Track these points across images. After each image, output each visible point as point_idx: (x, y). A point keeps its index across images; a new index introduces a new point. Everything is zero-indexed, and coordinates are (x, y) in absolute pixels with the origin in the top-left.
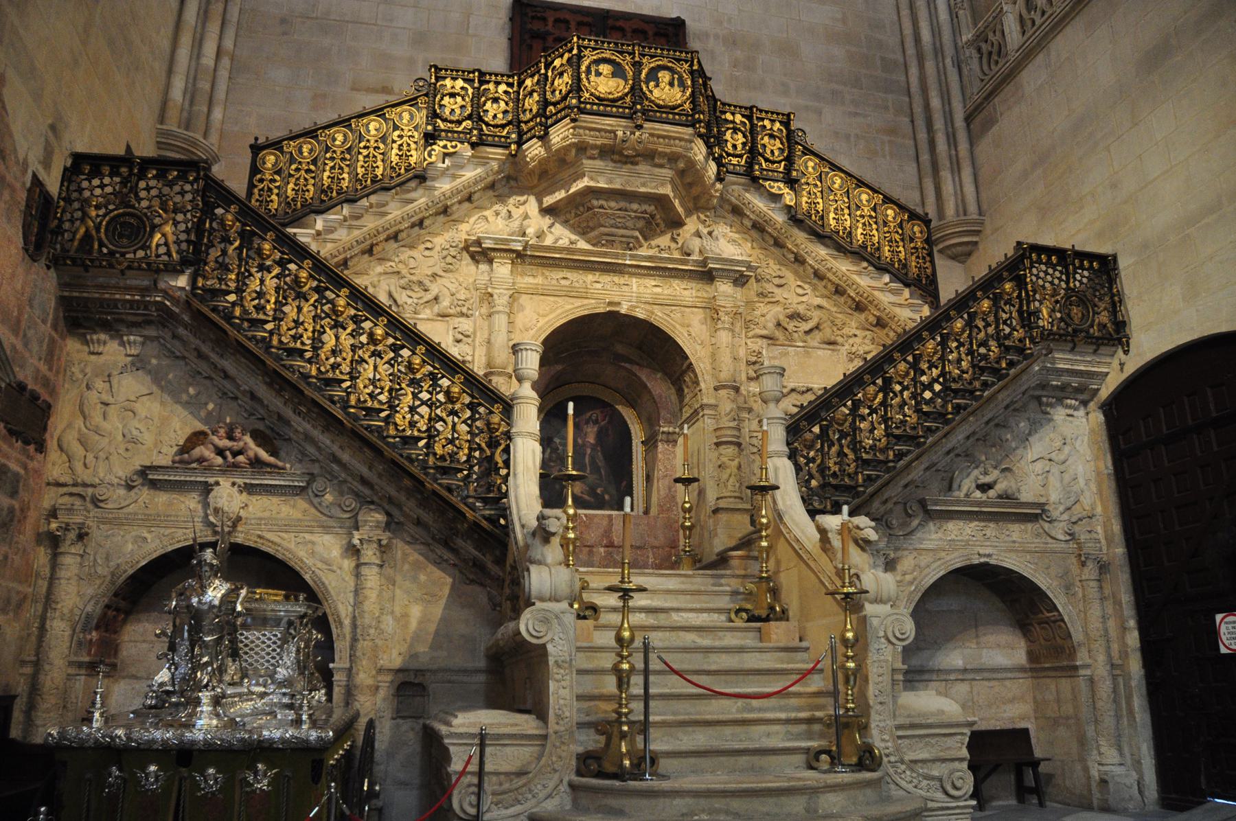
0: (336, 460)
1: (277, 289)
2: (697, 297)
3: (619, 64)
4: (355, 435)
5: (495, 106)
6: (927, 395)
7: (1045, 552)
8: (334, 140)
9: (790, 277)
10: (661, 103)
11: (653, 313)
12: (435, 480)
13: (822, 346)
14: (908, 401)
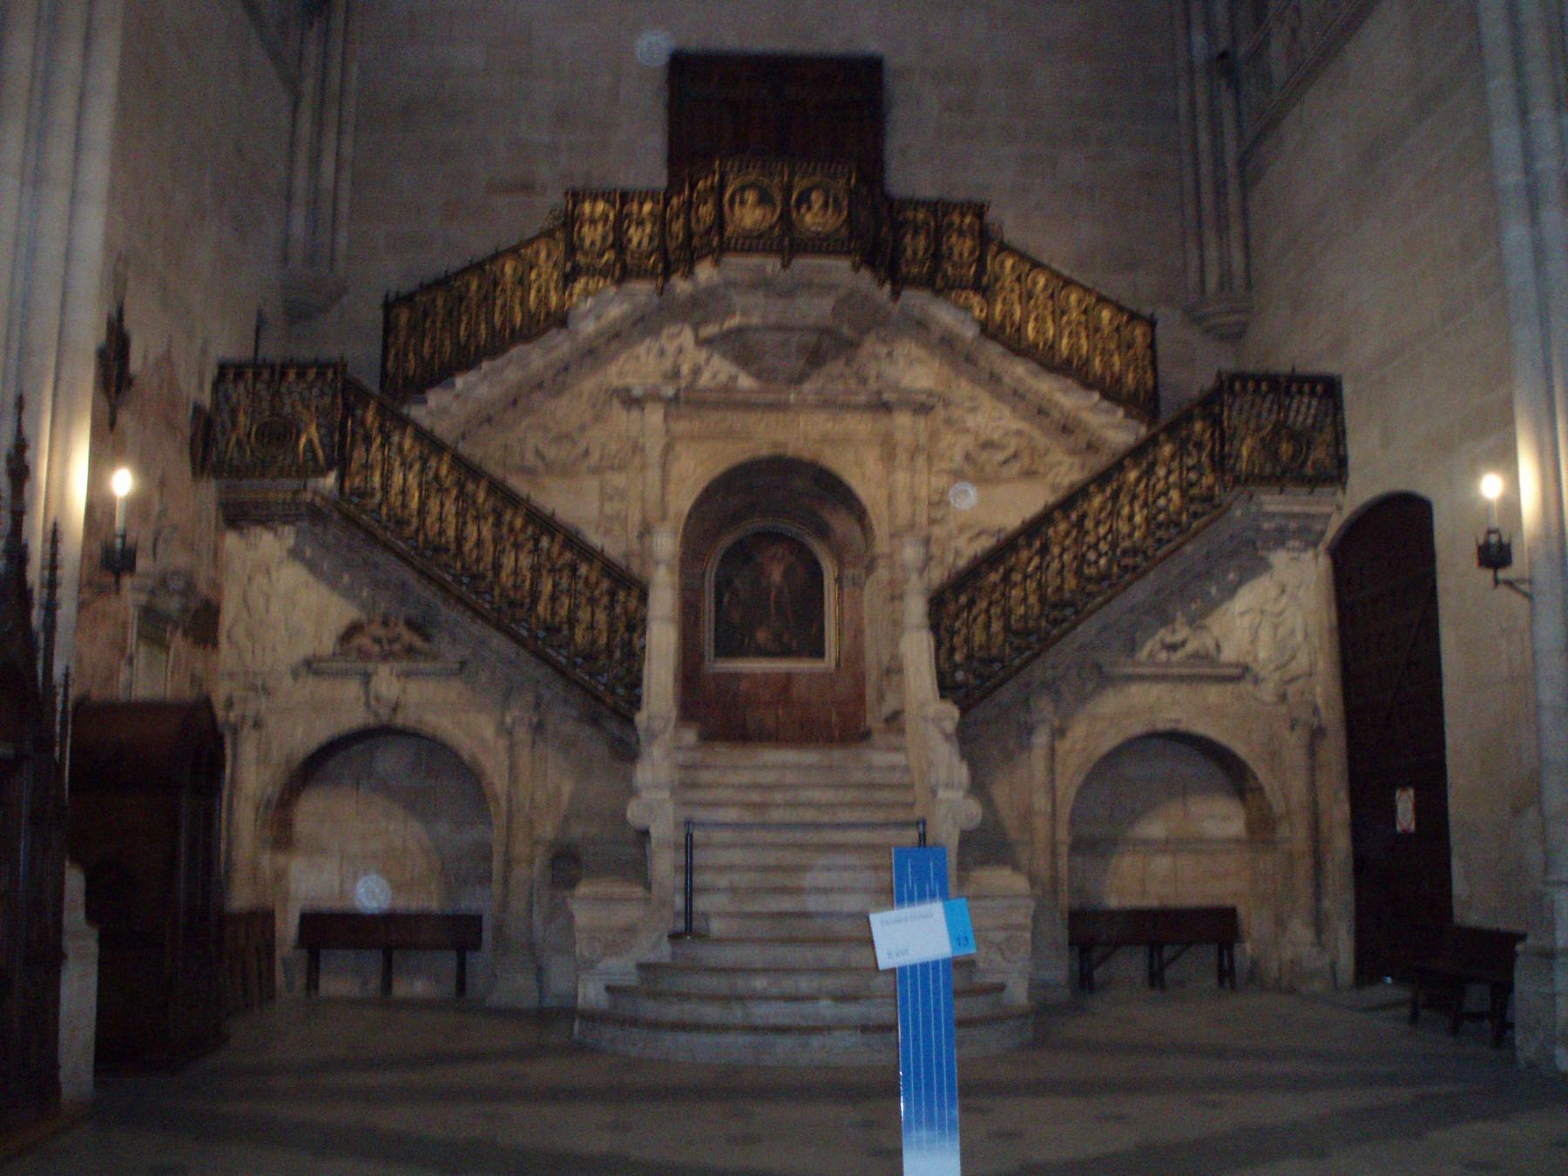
9: (986, 401)
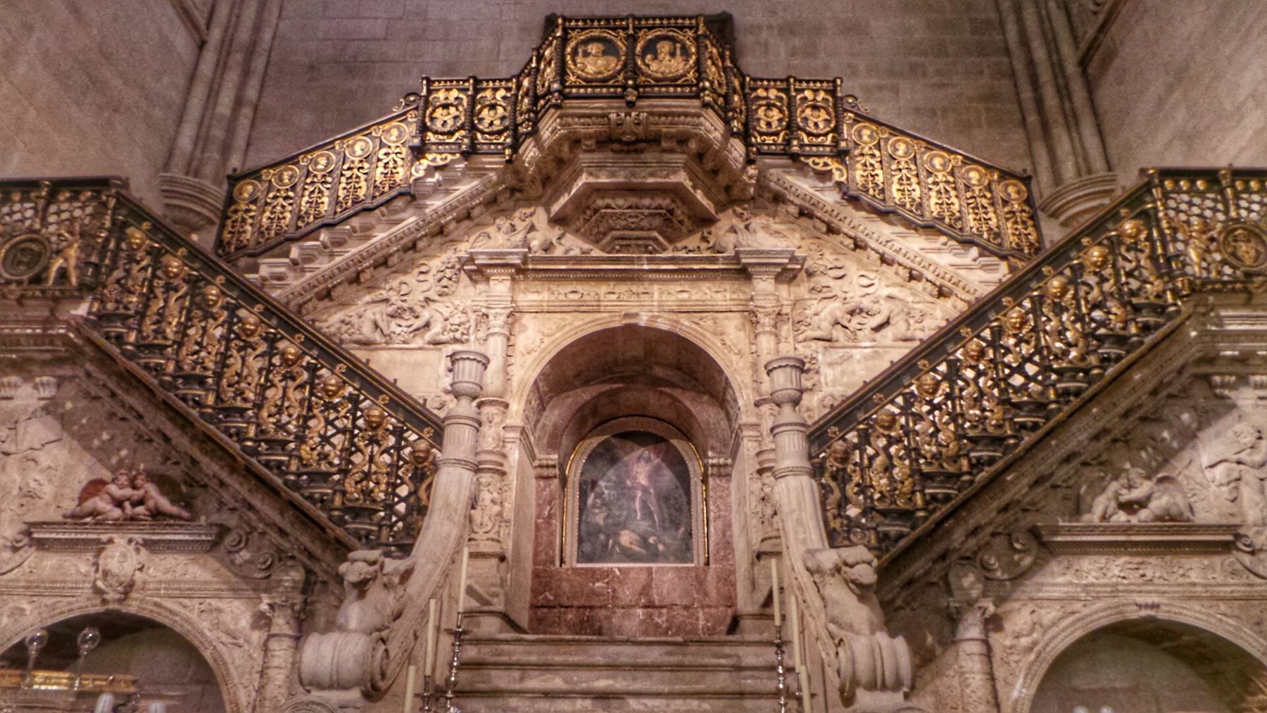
0: (251, 507)
2: (732, 300)
3: (610, 41)
4: (250, 473)
5: (492, 113)
6: (1018, 380)
8: (317, 163)
10: (659, 75)
11: (677, 322)
12: (341, 522)
13: (896, 344)
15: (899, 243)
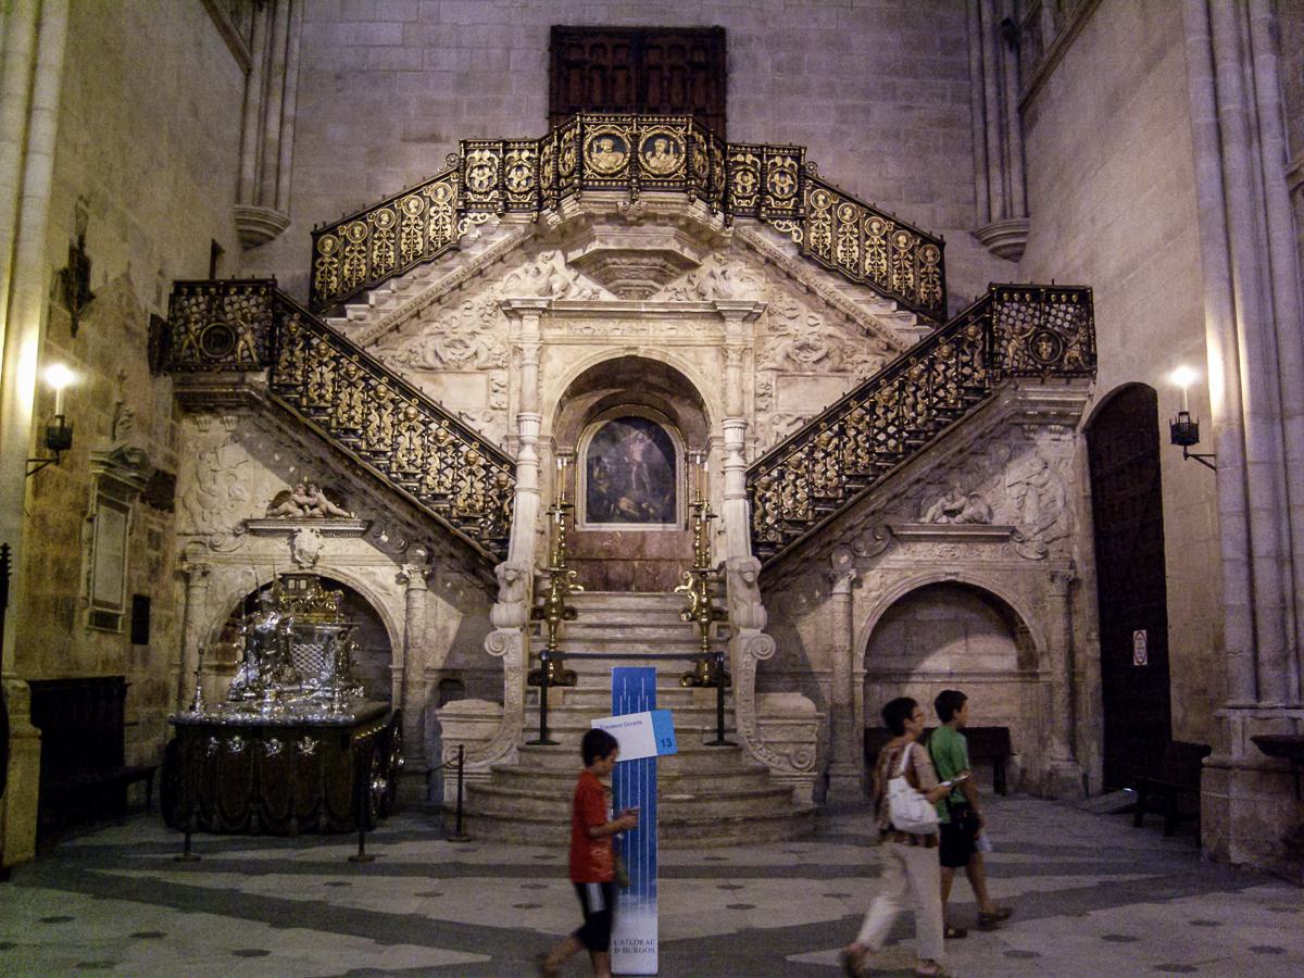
0: (386, 508)
1: (333, 380)
4: (396, 493)
6: (882, 437)
7: (1014, 570)
8: (380, 220)
9: (803, 309)
10: (656, 172)
12: (457, 526)
14: (861, 444)
15: (841, 295)
